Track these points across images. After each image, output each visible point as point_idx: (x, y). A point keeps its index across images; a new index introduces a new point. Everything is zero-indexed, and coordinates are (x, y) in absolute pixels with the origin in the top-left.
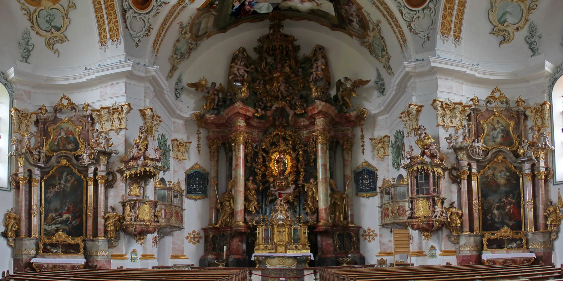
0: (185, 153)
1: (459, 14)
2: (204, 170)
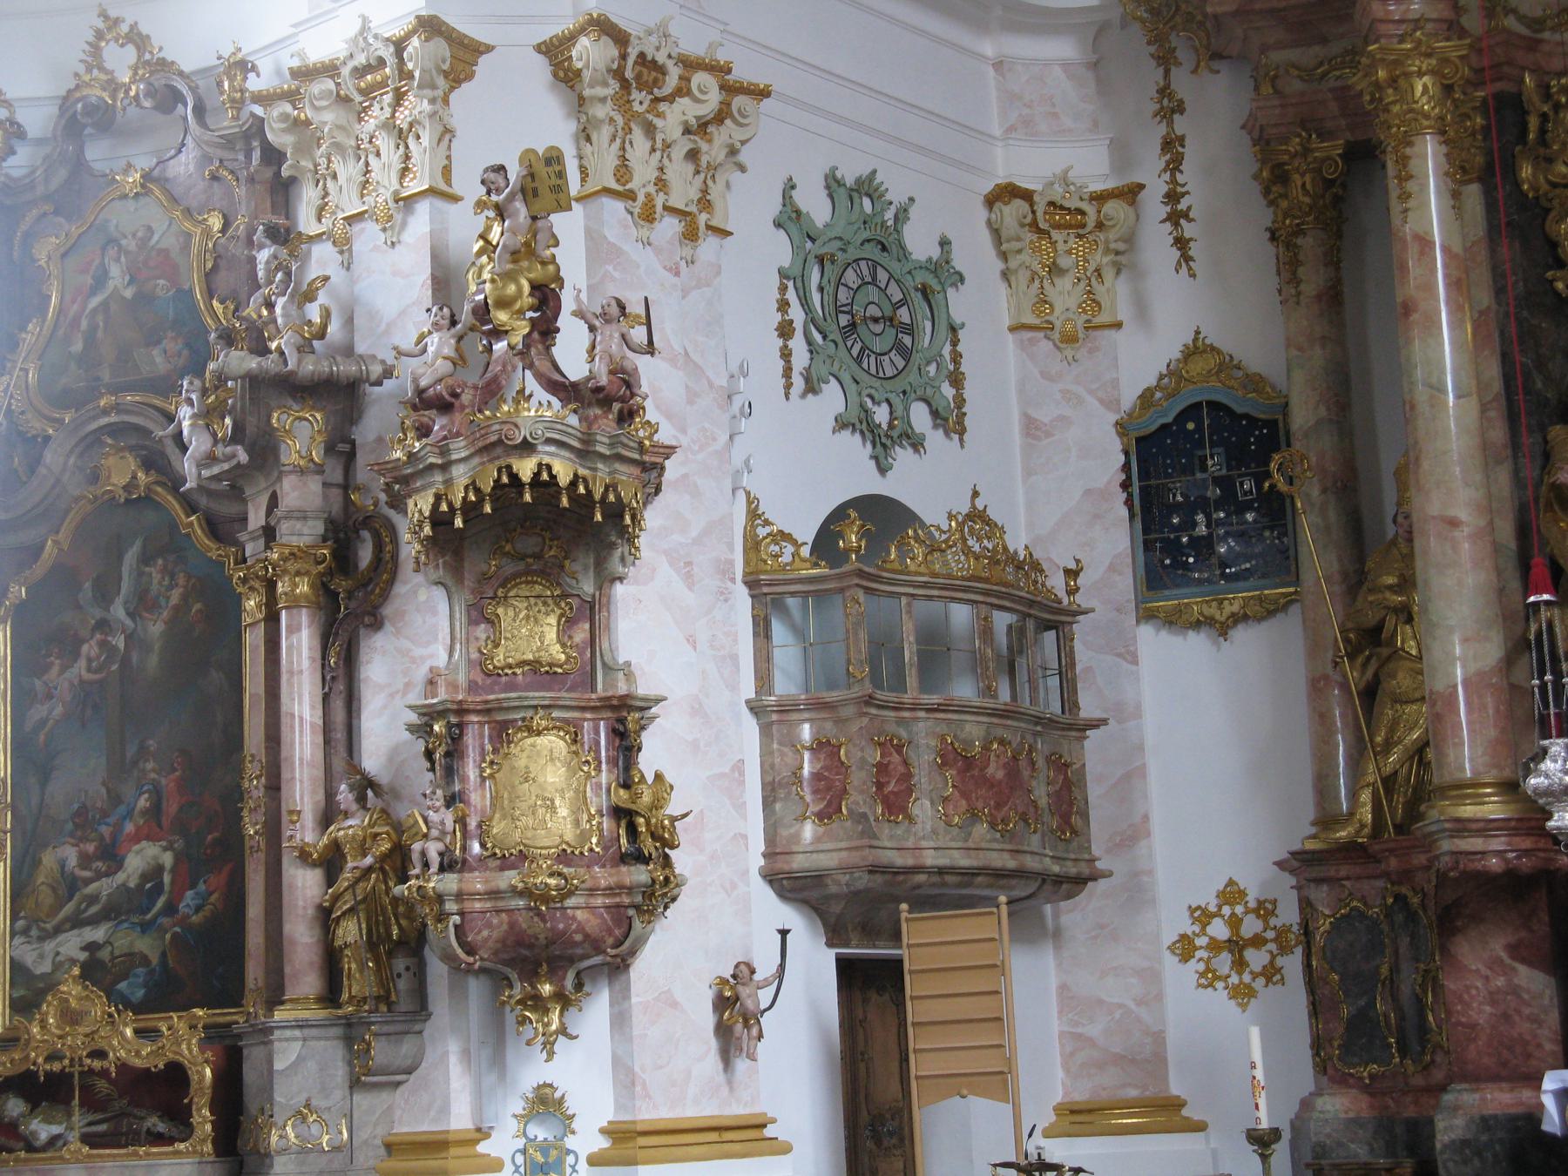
0: (1108, 274)
2: (1255, 382)
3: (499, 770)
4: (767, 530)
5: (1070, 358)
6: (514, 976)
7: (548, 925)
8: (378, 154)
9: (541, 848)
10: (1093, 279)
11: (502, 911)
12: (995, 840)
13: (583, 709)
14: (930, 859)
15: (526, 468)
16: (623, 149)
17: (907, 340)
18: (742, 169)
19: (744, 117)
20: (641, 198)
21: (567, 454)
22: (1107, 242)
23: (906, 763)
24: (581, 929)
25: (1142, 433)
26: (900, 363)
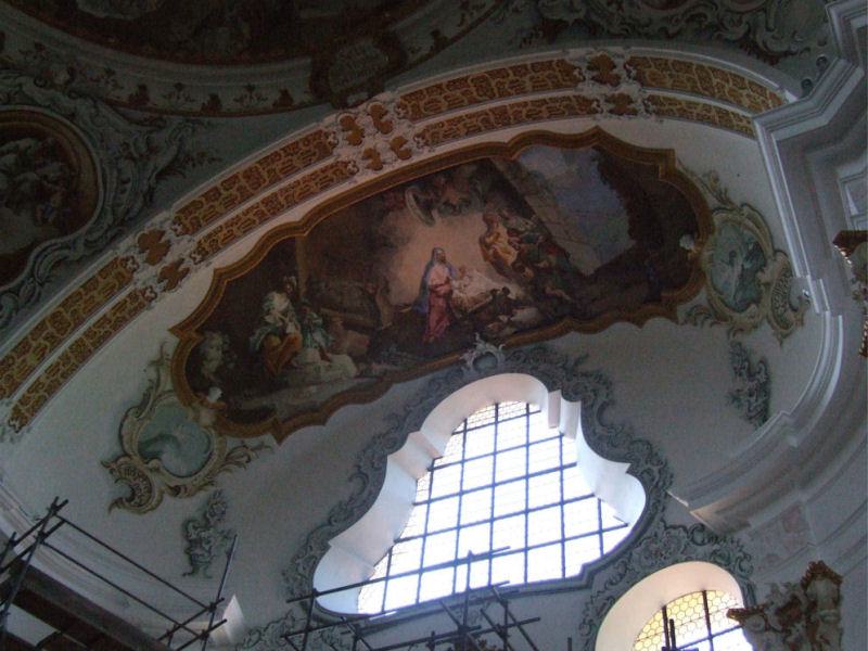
1: (61, 367)
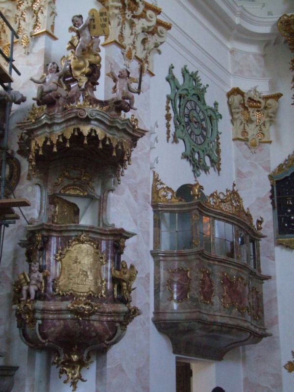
0: (267, 125)
3: (63, 258)
4: (162, 186)
5: (253, 152)
6: (61, 351)
7: (82, 327)
8: (24, 21)
9: (81, 293)
10: (262, 126)
11: (62, 319)
12: (239, 316)
13: (101, 234)
14: (219, 320)
15: (86, 130)
16: (122, 30)
17: (205, 133)
18: (159, 52)
19: (162, 33)
20: (127, 49)
21: (103, 127)
22: (268, 113)
23: (210, 281)
24: (95, 331)
25: (278, 179)
26: (203, 141)
